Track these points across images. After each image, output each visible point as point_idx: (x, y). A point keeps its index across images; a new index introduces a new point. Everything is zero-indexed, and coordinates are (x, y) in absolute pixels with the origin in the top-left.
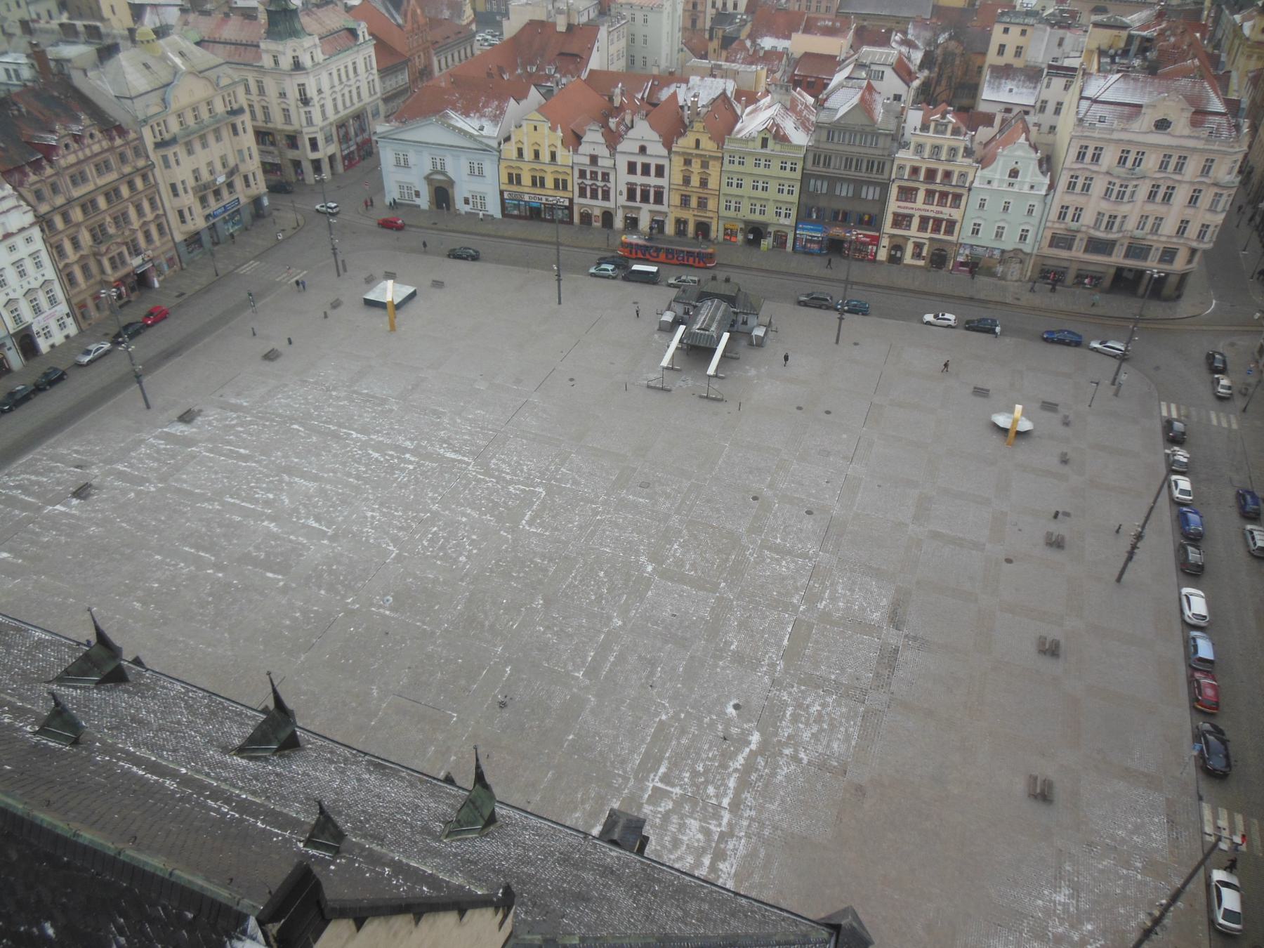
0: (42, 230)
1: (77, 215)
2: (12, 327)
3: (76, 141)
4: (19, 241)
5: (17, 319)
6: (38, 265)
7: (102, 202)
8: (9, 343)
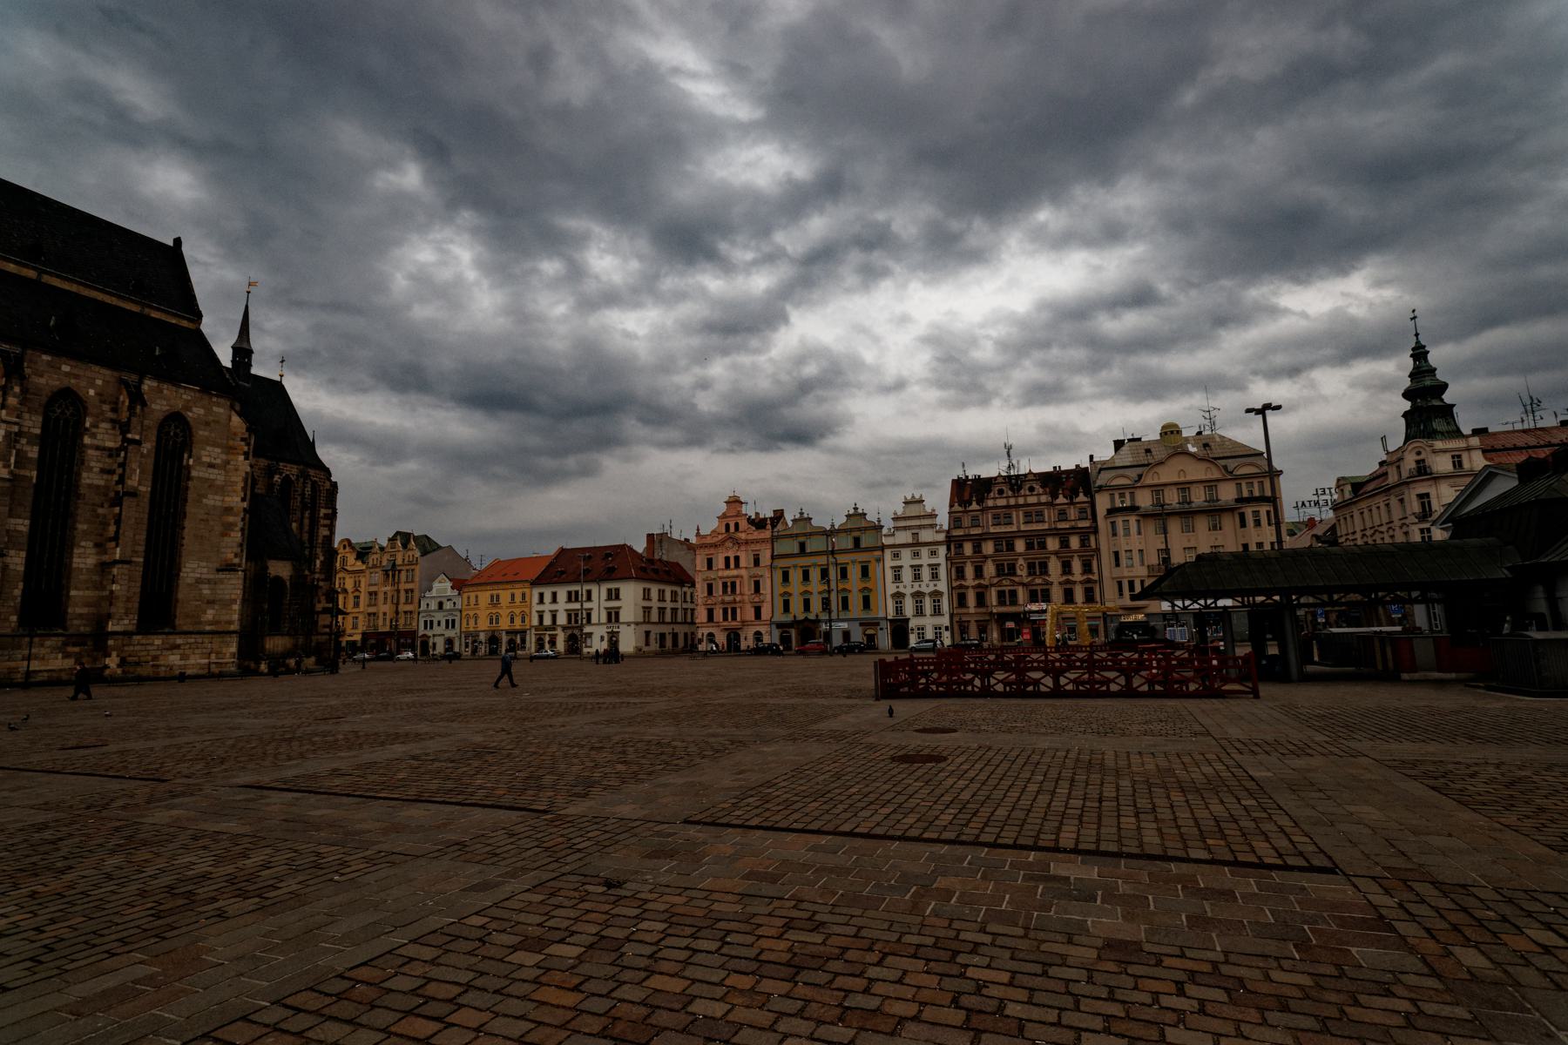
0: (949, 549)
1: (988, 548)
2: (891, 614)
3: (1012, 489)
4: (925, 551)
5: (899, 610)
6: (935, 576)
7: (1020, 546)
8: (883, 624)
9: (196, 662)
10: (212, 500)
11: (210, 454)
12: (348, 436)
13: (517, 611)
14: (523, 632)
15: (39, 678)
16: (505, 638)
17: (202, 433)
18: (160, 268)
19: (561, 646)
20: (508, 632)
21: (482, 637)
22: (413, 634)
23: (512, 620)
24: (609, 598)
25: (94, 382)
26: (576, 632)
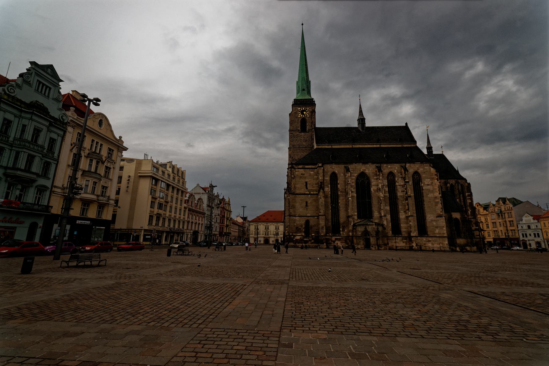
9: (436, 246)
10: (431, 195)
11: (427, 181)
12: (470, 166)
15: (399, 248)
17: (423, 176)
18: (404, 133)
22: (518, 239)
25: (395, 168)
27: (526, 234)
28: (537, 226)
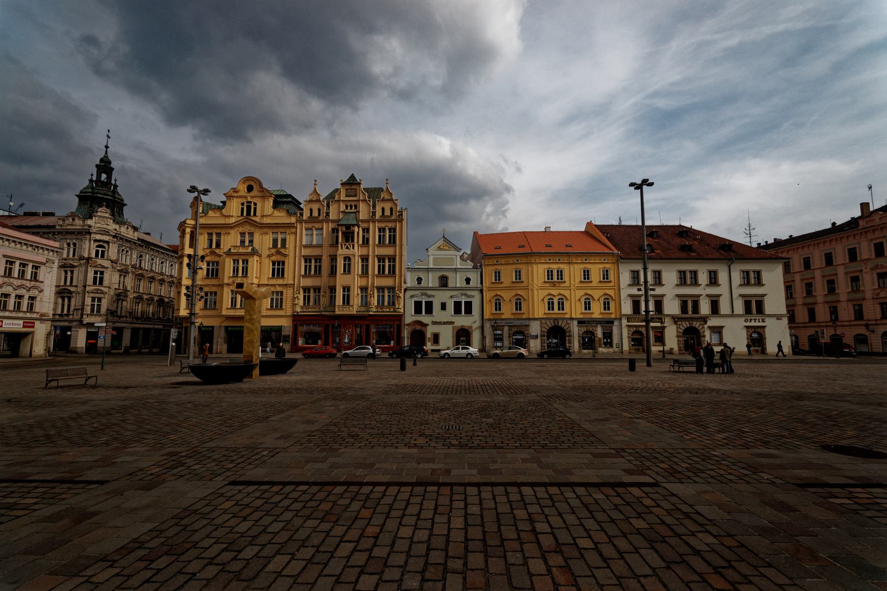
13: (597, 294)
14: (608, 323)
16: (576, 330)
19: (672, 340)
20: (581, 322)
21: (535, 328)
23: (588, 306)
24: (747, 283)
26: (696, 324)
27: (429, 305)
28: (468, 280)
